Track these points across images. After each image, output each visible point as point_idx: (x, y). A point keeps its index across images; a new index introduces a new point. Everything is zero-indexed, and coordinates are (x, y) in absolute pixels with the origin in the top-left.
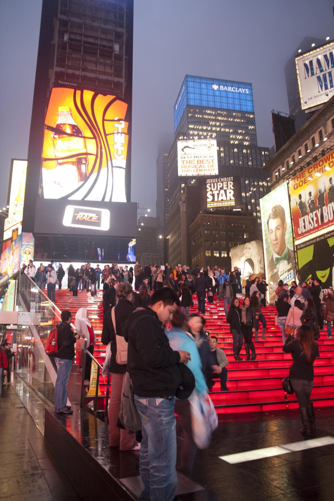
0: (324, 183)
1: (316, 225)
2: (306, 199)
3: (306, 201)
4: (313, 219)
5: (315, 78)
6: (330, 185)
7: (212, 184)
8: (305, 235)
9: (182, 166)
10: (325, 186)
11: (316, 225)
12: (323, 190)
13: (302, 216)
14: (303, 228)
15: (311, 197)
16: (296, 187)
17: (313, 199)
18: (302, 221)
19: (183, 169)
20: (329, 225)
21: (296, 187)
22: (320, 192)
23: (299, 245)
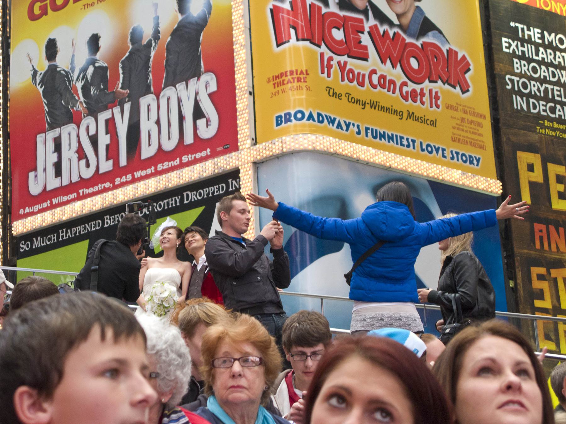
0: (156, 5)
1: (106, 166)
2: (73, 58)
3: (73, 69)
4: (94, 140)
6: (180, 17)
8: (55, 201)
10: (157, 18)
11: (106, 166)
12: (147, 34)
13: (52, 127)
14: (51, 171)
15: (98, 56)
16: (37, 11)
17: (105, 65)
18: (51, 146)
20: (160, 167)
21: (37, 11)
22: (133, 41)
23: (29, 236)
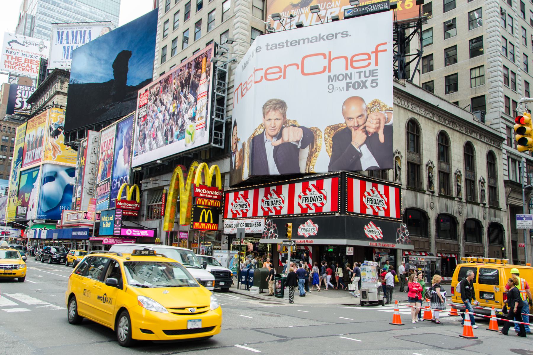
5: (62, 46)
7: (24, 92)
9: (5, 61)
19: (6, 64)
